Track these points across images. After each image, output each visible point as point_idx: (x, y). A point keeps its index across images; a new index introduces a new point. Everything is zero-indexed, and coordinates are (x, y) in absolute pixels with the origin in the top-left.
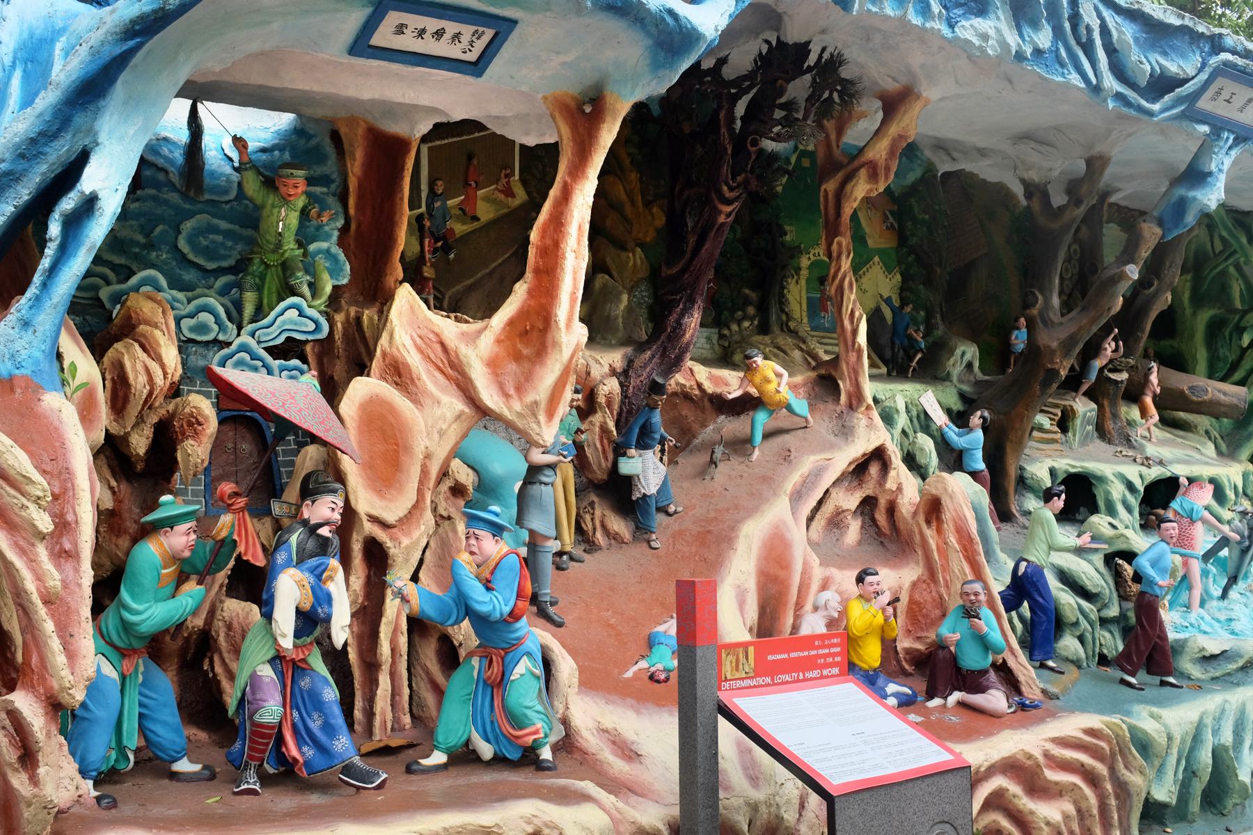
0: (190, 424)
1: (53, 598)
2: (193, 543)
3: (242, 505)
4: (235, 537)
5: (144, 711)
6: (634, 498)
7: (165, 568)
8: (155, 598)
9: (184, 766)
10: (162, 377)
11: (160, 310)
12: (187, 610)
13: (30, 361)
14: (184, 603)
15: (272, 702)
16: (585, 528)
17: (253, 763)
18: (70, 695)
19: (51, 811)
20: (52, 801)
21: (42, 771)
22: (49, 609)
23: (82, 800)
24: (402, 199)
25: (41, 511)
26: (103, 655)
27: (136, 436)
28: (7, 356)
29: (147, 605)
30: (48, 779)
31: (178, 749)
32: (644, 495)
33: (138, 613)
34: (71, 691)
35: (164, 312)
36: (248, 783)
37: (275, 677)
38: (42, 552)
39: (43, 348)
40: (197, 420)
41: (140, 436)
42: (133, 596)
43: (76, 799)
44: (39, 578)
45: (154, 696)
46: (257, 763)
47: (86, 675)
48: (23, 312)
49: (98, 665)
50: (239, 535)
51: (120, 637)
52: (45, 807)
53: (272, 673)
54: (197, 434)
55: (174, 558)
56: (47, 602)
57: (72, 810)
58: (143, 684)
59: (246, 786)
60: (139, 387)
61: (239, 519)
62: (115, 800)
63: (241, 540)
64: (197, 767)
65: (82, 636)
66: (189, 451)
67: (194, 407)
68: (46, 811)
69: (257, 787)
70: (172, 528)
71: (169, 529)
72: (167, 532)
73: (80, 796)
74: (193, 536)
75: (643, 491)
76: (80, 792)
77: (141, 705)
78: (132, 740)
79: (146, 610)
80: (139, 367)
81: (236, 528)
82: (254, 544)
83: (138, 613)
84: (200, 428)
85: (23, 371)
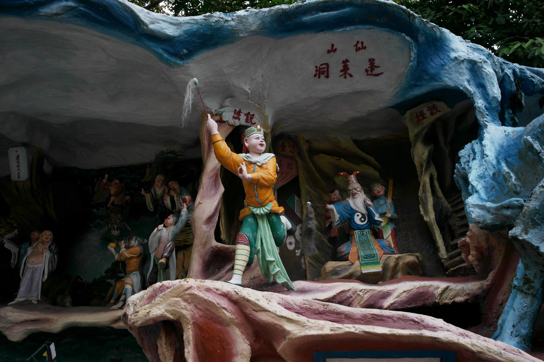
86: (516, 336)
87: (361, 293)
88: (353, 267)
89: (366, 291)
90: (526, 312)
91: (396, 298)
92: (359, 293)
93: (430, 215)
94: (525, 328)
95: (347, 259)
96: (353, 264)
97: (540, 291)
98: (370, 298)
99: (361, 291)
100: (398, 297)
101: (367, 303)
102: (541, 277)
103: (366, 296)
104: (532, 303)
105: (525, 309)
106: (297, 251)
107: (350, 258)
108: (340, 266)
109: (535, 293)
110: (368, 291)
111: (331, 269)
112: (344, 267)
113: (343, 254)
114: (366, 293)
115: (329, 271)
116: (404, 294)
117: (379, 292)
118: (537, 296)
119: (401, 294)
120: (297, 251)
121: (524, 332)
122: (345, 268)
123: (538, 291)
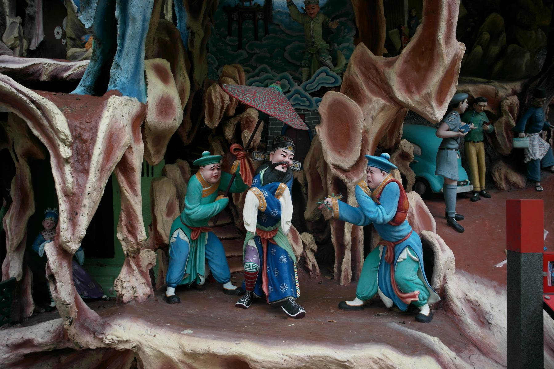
0: (247, 122)
1: (69, 193)
2: (216, 175)
3: (242, 155)
4: (240, 173)
5: (208, 257)
6: (525, 162)
7: (204, 187)
8: (200, 201)
9: (229, 286)
10: (228, 99)
11: (237, 71)
12: (217, 209)
13: (121, 83)
14: (215, 206)
15: (251, 260)
16: (495, 180)
17: (248, 291)
18: (68, 246)
19: (67, 306)
20: (65, 301)
21: (58, 284)
22: (69, 199)
23: (137, 299)
24: (380, 13)
25: (66, 147)
26: (181, 229)
27: (228, 130)
28: (113, 82)
29: (194, 205)
30: (62, 289)
31: (223, 278)
32: (532, 159)
33: (190, 209)
34: (68, 244)
35: (239, 72)
36: (240, 302)
37: (256, 247)
38: (68, 169)
39: (126, 76)
40: (250, 120)
41: (229, 130)
42: (188, 201)
43: (133, 298)
44: (64, 181)
45: (212, 251)
46: (250, 291)
47: (79, 236)
48: (116, 59)
49: (179, 233)
50: (242, 171)
51: (187, 221)
52: (63, 304)
53: (255, 245)
54: (250, 127)
55: (206, 183)
56: (67, 194)
57: (130, 303)
58: (206, 245)
59: (238, 303)
60: (217, 104)
61: (241, 163)
62: (179, 299)
63: (242, 174)
64: (234, 288)
65: (81, 215)
66: (246, 135)
67: (248, 114)
68: (64, 306)
69: (244, 304)
70: (204, 167)
71: (203, 167)
72: (202, 169)
73: (136, 297)
74: (216, 171)
75: (531, 157)
76: (136, 295)
77: (206, 254)
78: (202, 271)
79: (194, 208)
80: (218, 95)
81: (240, 167)
82: (249, 176)
83: (190, 209)
84: (251, 124)
85: (117, 88)
86: (83, 86)
87: (45, 66)
88: (87, 53)
89: (50, 64)
90: (90, 71)
91: (73, 71)
92: (44, 65)
93: (169, 14)
94: (89, 82)
95: (84, 47)
96: (87, 51)
97: (100, 58)
98: (54, 70)
99: (45, 64)
100: (75, 70)
101: (51, 74)
102: (100, 48)
103: (51, 69)
104: (95, 65)
105: (90, 69)
106: (63, 40)
107: (86, 46)
108: (78, 52)
109: (96, 59)
110: (52, 65)
111: (71, 54)
112: (81, 53)
113: (83, 42)
114: (50, 66)
115: (69, 56)
116: (80, 68)
117: (63, 66)
118: (98, 61)
119: (78, 68)
120: (63, 40)
121: (88, 84)
122: (82, 54)
123: (99, 57)
